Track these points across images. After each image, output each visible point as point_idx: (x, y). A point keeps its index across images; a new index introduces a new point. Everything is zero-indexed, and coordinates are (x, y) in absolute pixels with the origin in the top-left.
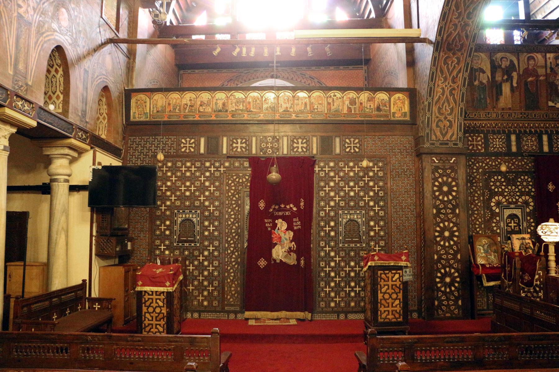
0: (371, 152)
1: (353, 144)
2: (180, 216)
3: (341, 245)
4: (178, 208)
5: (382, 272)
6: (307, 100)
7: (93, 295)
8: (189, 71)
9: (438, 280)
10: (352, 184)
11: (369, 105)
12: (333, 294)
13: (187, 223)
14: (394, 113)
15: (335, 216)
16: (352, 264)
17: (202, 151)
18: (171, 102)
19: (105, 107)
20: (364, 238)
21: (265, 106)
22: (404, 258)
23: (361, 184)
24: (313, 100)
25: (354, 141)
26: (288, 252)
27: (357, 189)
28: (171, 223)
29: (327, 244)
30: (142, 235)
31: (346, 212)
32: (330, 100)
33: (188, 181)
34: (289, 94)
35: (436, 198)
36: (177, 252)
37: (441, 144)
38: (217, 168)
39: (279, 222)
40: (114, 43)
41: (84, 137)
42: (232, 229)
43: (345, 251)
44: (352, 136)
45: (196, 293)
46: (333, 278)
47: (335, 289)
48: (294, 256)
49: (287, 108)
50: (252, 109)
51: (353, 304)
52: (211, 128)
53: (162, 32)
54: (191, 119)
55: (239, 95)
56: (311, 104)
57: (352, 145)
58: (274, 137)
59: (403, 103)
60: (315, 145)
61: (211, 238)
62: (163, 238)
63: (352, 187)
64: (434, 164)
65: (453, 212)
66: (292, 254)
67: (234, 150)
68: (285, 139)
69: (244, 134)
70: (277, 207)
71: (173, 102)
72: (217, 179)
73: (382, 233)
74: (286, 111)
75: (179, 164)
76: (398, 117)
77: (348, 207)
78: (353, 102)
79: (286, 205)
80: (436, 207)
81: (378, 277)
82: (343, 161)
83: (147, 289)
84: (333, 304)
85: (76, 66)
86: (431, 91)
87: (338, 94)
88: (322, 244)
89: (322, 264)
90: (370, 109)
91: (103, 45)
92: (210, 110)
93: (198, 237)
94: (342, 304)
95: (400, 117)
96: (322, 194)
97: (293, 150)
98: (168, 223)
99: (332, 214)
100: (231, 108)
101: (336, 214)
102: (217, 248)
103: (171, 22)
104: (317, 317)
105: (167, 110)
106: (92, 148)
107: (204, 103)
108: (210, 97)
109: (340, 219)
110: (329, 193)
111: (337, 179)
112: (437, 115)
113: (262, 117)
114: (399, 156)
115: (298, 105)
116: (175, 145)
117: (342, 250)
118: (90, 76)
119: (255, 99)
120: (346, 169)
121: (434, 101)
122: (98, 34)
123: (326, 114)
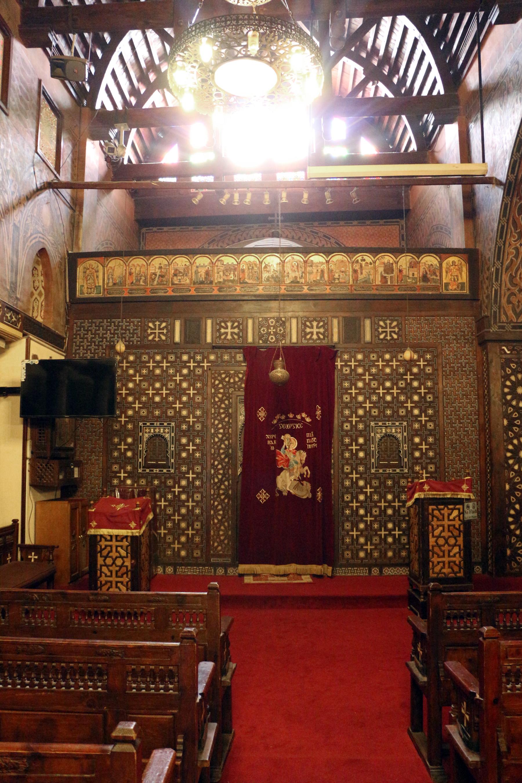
0: (415, 339)
1: (389, 328)
2: (147, 430)
3: (373, 471)
4: (144, 419)
5: (435, 507)
6: (325, 267)
7: (27, 542)
8: (155, 229)
9: (510, 519)
10: (388, 384)
11: (411, 273)
12: (362, 540)
13: (157, 440)
14: (447, 285)
15: (365, 430)
16: (390, 497)
17: (177, 339)
18: (133, 271)
19: (42, 278)
20: (406, 460)
21: (265, 275)
22: (465, 487)
23: (402, 384)
24: (332, 267)
25: (390, 324)
26: (299, 480)
27: (395, 391)
28: (134, 440)
29: (354, 468)
30: (94, 457)
31: (380, 424)
32: (357, 267)
33: (158, 380)
34: (299, 258)
35: (508, 403)
36: (143, 482)
37: (514, 327)
38: (199, 362)
39: (287, 438)
40: (53, 188)
41: (14, 319)
42: (219, 448)
43: (379, 478)
44: (388, 317)
45: (170, 539)
46: (362, 516)
47: (365, 533)
48: (307, 485)
49: (296, 277)
50: (247, 280)
51: (390, 554)
52: (190, 306)
53: (118, 173)
54: (161, 294)
55: (229, 260)
56: (330, 271)
57: (388, 330)
58: (278, 319)
59: (460, 270)
60: (335, 330)
61: (190, 462)
62: (123, 461)
63: (388, 389)
64: (504, 356)
66: (305, 483)
67: (223, 337)
68: (294, 321)
69: (237, 315)
70: (283, 417)
71: (135, 271)
72: (199, 378)
73: (431, 454)
74: (295, 281)
75: (145, 358)
76: (453, 289)
77: (382, 417)
78: (389, 269)
79: (295, 414)
80: (506, 415)
81: (429, 514)
82: (376, 352)
83: (104, 531)
84: (362, 554)
85: (3, 220)
86: (499, 253)
87: (368, 258)
88: (347, 469)
89: (347, 497)
90: (414, 279)
91: (39, 190)
92: (188, 281)
93: (173, 461)
94: (376, 554)
95: (455, 289)
96: (346, 398)
97: (305, 337)
98: (130, 440)
99: (361, 426)
100: (218, 277)
101: (367, 426)
102: (198, 476)
103: (129, 160)
104: (341, 572)
105: (128, 282)
106: (24, 335)
107: (180, 272)
108: (188, 264)
109: (372, 434)
110: (356, 398)
111: (367, 377)
112: (509, 285)
113: (261, 290)
114: (454, 345)
115: (311, 273)
116: (139, 331)
117: (376, 478)
118: (22, 234)
119: (250, 265)
120: (380, 363)
121: (505, 267)
122: (32, 176)
123: (351, 286)
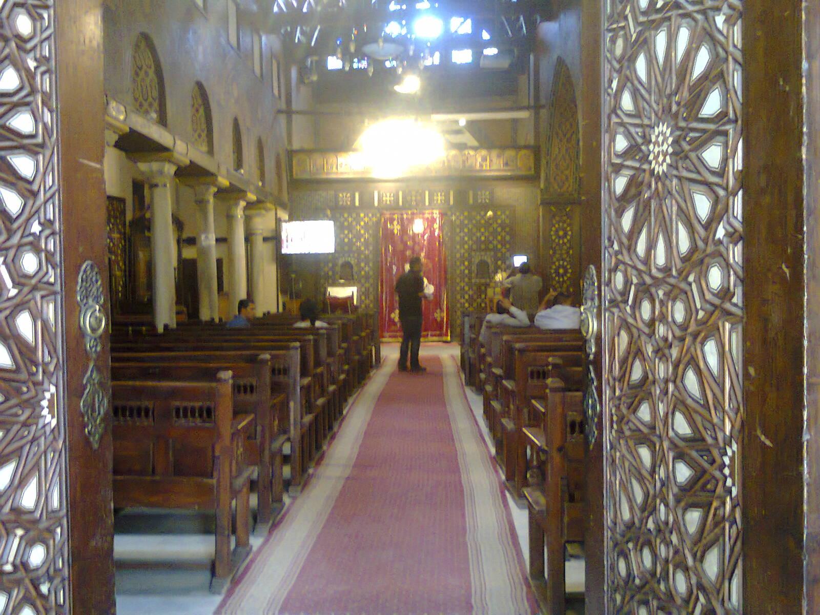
17: (357, 204)
23: (491, 229)
29: (462, 280)
65: (568, 253)
87: (472, 153)
